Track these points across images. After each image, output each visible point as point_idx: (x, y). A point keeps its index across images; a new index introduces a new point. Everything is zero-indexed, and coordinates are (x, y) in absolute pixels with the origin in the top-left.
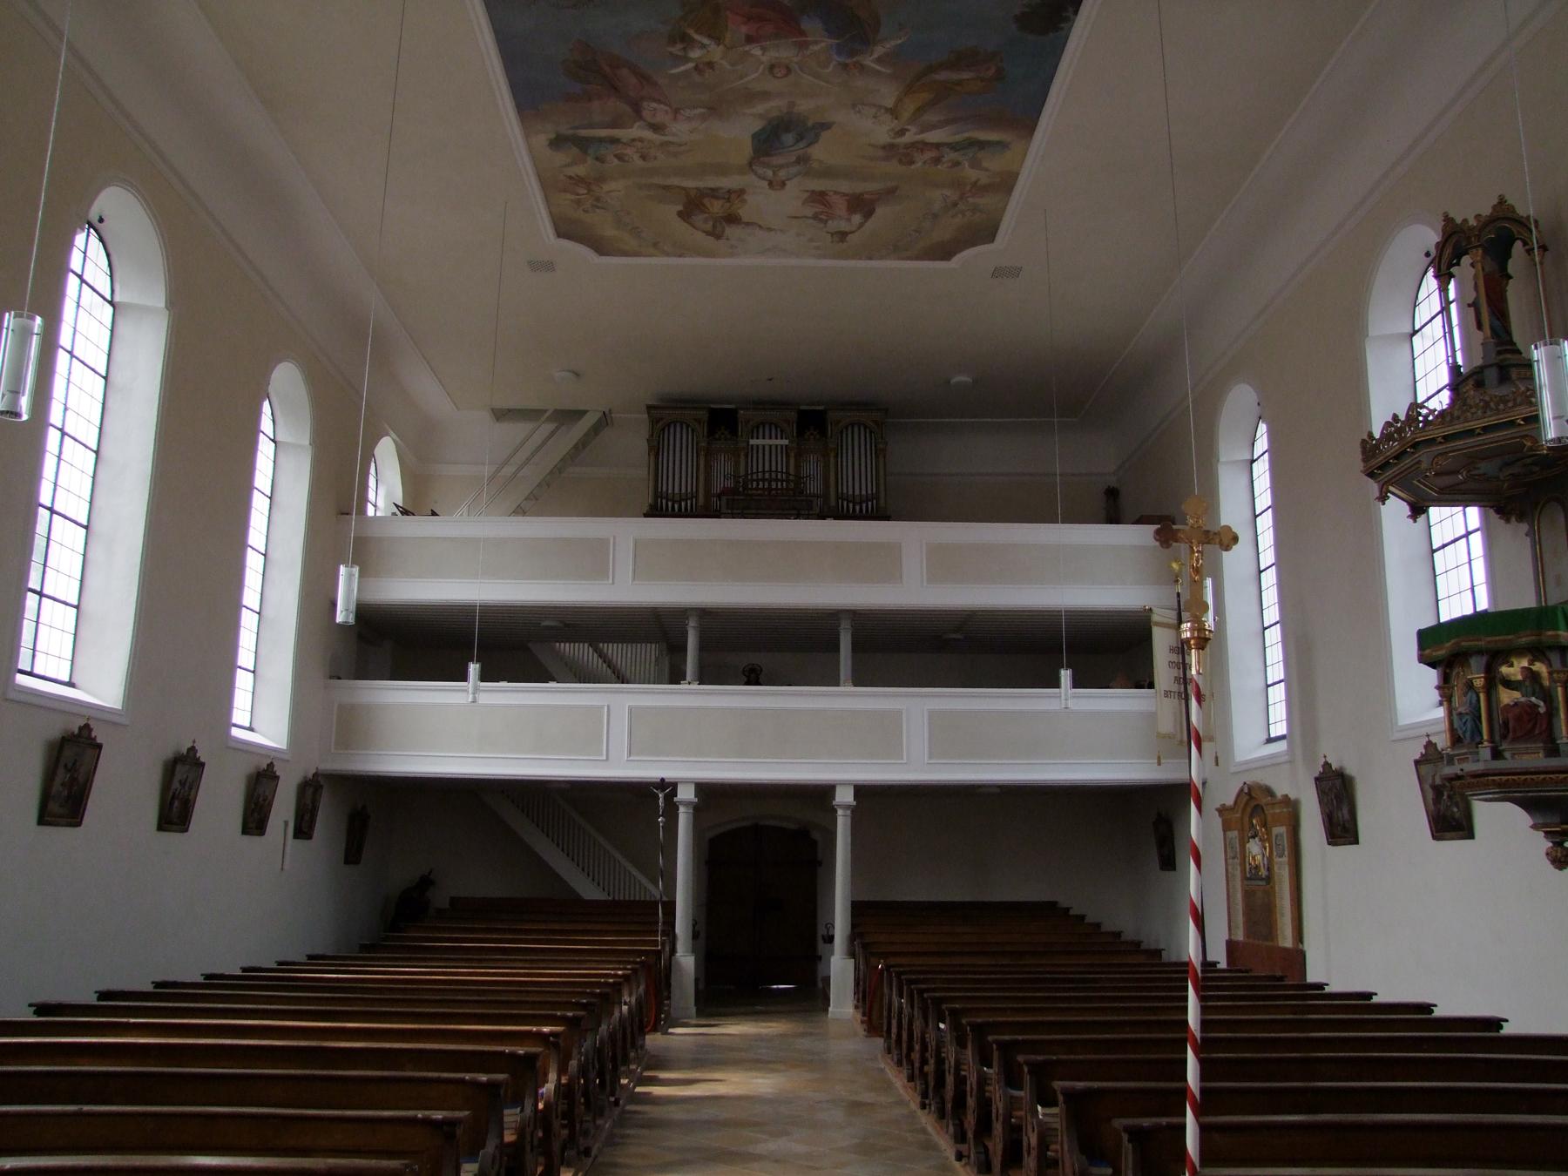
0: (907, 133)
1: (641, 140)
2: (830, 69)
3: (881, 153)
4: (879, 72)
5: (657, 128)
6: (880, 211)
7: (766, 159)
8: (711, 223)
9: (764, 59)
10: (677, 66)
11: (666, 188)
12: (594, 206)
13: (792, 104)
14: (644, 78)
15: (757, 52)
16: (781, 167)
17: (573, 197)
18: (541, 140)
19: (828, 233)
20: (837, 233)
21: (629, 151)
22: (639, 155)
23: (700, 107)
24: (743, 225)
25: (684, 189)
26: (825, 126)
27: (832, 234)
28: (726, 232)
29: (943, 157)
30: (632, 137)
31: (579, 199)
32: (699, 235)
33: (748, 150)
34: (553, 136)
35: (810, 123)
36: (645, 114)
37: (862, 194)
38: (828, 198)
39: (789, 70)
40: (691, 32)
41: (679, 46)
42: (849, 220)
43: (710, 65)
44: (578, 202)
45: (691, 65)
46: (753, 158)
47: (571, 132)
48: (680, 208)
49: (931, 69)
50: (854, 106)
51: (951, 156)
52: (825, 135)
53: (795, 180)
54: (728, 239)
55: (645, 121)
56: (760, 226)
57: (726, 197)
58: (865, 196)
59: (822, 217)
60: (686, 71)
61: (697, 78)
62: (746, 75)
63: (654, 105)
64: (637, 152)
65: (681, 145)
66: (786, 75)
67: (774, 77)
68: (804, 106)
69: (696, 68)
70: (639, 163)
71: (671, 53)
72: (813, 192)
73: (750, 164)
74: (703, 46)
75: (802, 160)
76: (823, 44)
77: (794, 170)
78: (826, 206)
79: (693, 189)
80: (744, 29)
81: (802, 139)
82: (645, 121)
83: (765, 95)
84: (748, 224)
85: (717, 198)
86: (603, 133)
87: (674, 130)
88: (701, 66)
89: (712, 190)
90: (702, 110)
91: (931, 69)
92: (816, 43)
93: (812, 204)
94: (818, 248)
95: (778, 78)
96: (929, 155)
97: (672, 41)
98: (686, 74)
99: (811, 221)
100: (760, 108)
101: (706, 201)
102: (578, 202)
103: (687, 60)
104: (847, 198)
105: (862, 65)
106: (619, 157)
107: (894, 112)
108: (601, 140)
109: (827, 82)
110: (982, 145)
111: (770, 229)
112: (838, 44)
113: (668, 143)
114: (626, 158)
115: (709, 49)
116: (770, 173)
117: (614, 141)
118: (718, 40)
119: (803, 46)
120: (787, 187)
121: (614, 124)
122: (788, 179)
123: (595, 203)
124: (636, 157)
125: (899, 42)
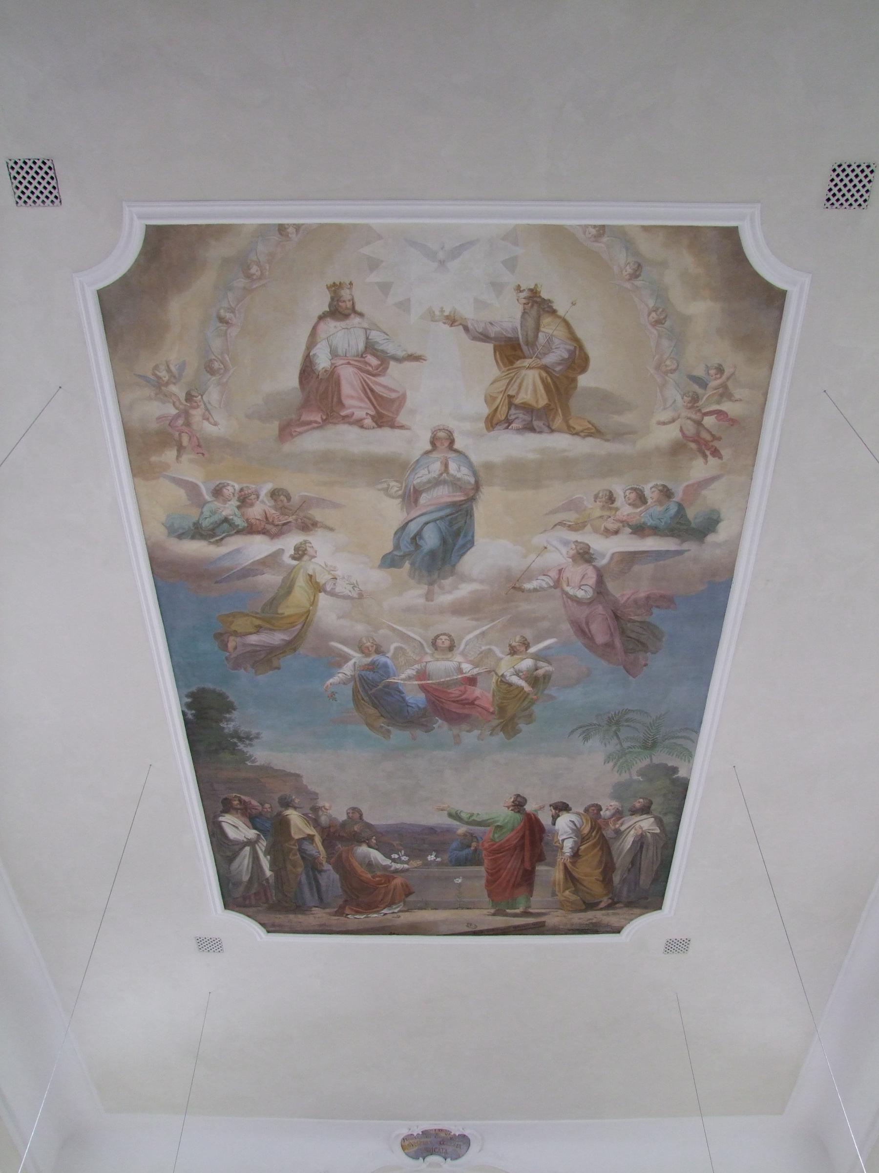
0: (292, 552)
1: (609, 533)
2: (393, 647)
3: (317, 514)
4: (344, 642)
5: (584, 555)
6: (290, 379)
7: (459, 497)
8: (541, 337)
9: (459, 658)
10: (548, 648)
11: (595, 432)
12: (703, 384)
13: (429, 596)
14: (582, 631)
15: (466, 667)
16: (437, 483)
17: (726, 406)
18: (723, 533)
19: (361, 315)
20: (346, 316)
21: (625, 510)
22: (615, 505)
23: (529, 591)
24: (492, 331)
25: (571, 431)
26: (390, 561)
27: (354, 311)
28: (519, 315)
29: (239, 507)
30: (615, 539)
31: (719, 403)
32: (561, 306)
33: (480, 512)
34: (710, 538)
35: (407, 565)
36: (592, 579)
37: (326, 422)
38: (373, 413)
39: (434, 644)
40: (527, 688)
41: (540, 672)
42: (334, 354)
43: (513, 651)
44: (725, 394)
45: (533, 650)
46: (472, 499)
47: (685, 546)
48: (584, 380)
49: (291, 646)
50: (361, 596)
51: (229, 509)
52: (389, 547)
53: (416, 454)
54: (518, 289)
55: (595, 567)
56: (466, 329)
57: (513, 411)
58: (317, 417)
59: (373, 361)
60: (539, 642)
61: (528, 634)
62: (477, 637)
63: (580, 594)
64: (617, 509)
65: (561, 524)
66: (437, 637)
67: (450, 636)
68: (415, 595)
69: (527, 646)
70: (619, 489)
71: (550, 663)
72: (393, 425)
73: (477, 487)
74: (517, 673)
75: (411, 497)
76: (403, 676)
77: (422, 476)
78: (372, 390)
79: (559, 431)
80: (477, 692)
81: (414, 538)
82: (595, 567)
83: (458, 609)
84: (484, 337)
85: (526, 408)
86: (651, 544)
87: (564, 550)
88: (523, 649)
89: (530, 428)
90: (528, 586)
91: (291, 646)
92: (410, 678)
93: (393, 395)
94: (374, 265)
95: (444, 634)
96: (256, 512)
97: (547, 677)
98: (539, 639)
99: (390, 348)
100: (465, 590)
101: (543, 401)
102: (725, 394)
103: (537, 657)
104: (343, 413)
105: (362, 652)
106: (641, 499)
107: (318, 588)
108: (656, 531)
109: (394, 630)
110: (198, 532)
111: (452, 320)
112: (388, 677)
113: (575, 527)
114: (633, 496)
115: (512, 670)
116: (453, 467)
117: (640, 530)
118: (503, 681)
119: (422, 675)
120: (428, 436)
121: (630, 559)
122: (427, 453)
123: (700, 391)
124: (620, 502)
125: (331, 681)
